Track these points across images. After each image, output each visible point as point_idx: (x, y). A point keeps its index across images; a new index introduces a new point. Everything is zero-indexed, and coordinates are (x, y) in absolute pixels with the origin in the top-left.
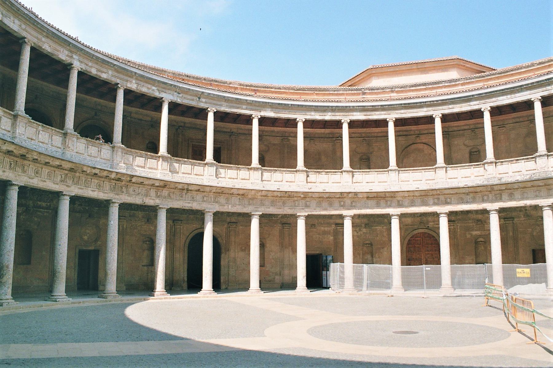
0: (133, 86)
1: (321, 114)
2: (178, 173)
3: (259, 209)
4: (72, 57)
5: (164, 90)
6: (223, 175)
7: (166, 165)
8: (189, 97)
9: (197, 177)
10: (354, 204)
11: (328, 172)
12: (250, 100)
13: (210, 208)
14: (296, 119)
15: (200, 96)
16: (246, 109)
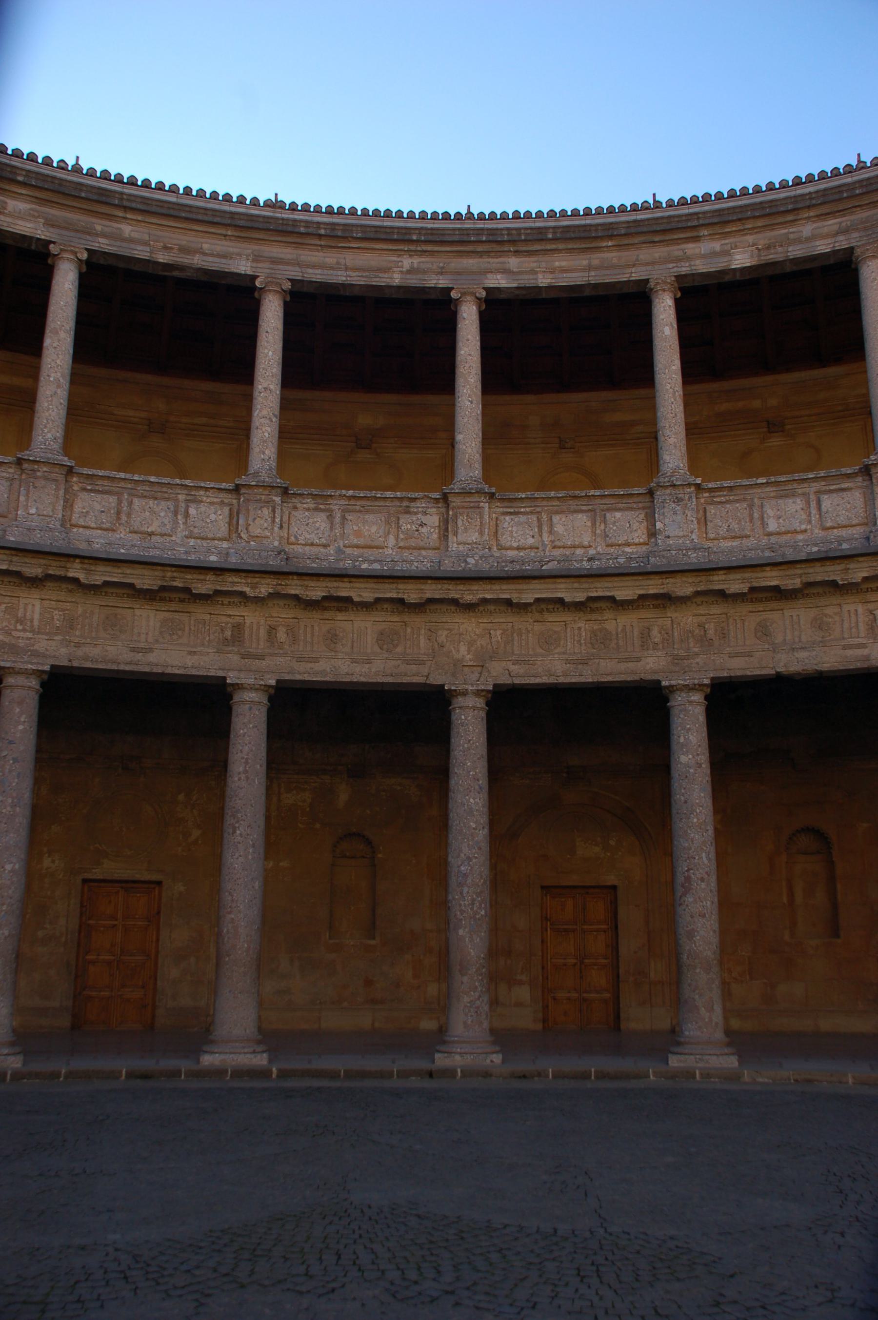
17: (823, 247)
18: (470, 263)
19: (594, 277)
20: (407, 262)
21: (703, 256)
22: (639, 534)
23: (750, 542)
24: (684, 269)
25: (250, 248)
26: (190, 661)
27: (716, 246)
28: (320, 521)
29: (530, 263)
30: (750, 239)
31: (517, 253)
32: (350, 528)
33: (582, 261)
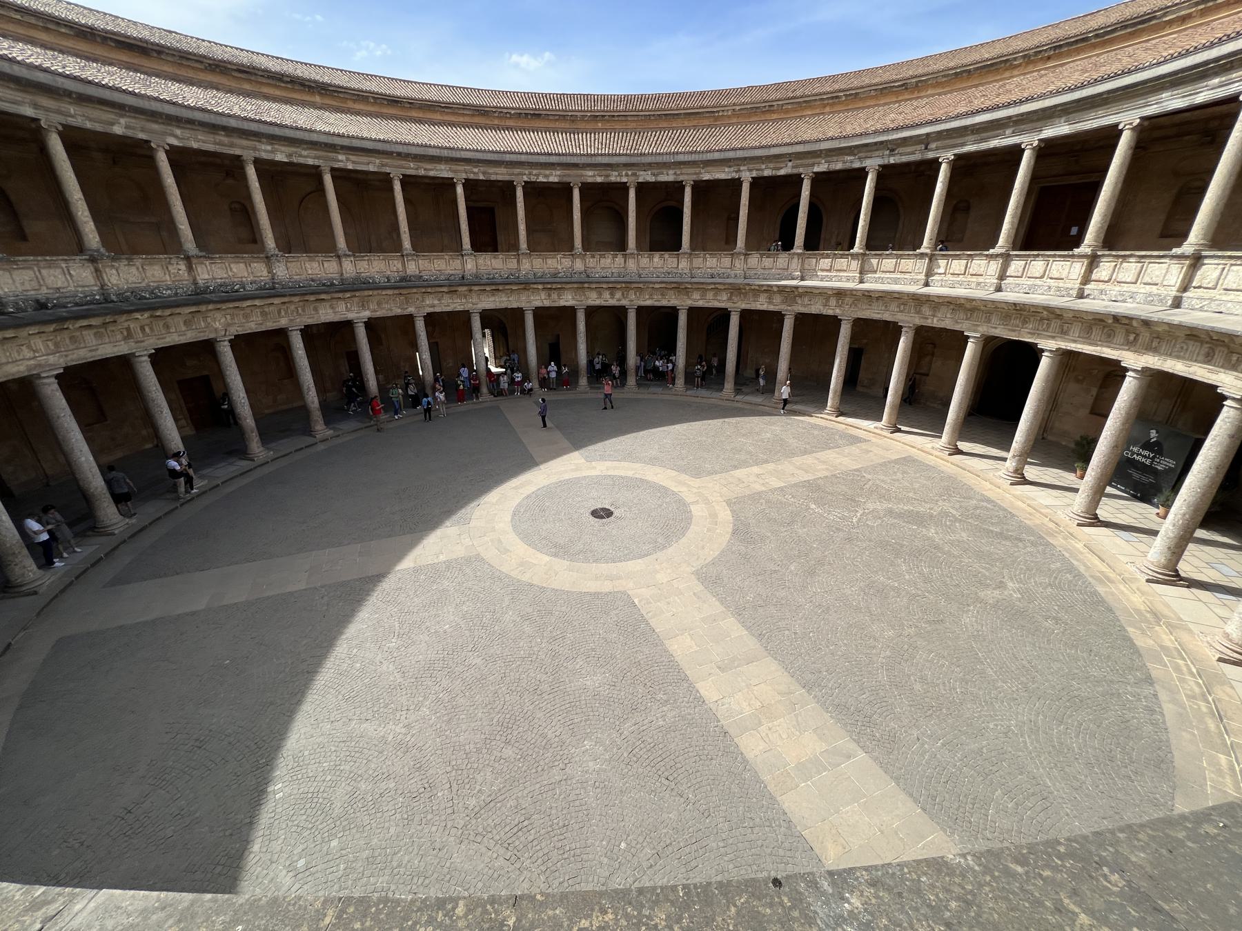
0: (822, 167)
1: (1189, 89)
2: (875, 272)
3: (980, 329)
4: (739, 171)
5: (869, 154)
6: (941, 270)
7: (855, 264)
8: (909, 149)
9: (902, 276)
10: (1154, 344)
11: (1143, 257)
12: (1017, 115)
13: (909, 320)
14: (1117, 125)
15: (926, 140)
16: (1014, 134)
17: (310, 162)
18: (155, 127)
19: (218, 149)
20: (122, 121)
21: (265, 151)
22: (265, 273)
23: (303, 277)
24: (257, 155)
25: (28, 98)
26: (116, 349)
27: (269, 148)
28: (133, 270)
29: (187, 134)
30: (283, 149)
31: (178, 127)
32: (149, 274)
33: (211, 138)
